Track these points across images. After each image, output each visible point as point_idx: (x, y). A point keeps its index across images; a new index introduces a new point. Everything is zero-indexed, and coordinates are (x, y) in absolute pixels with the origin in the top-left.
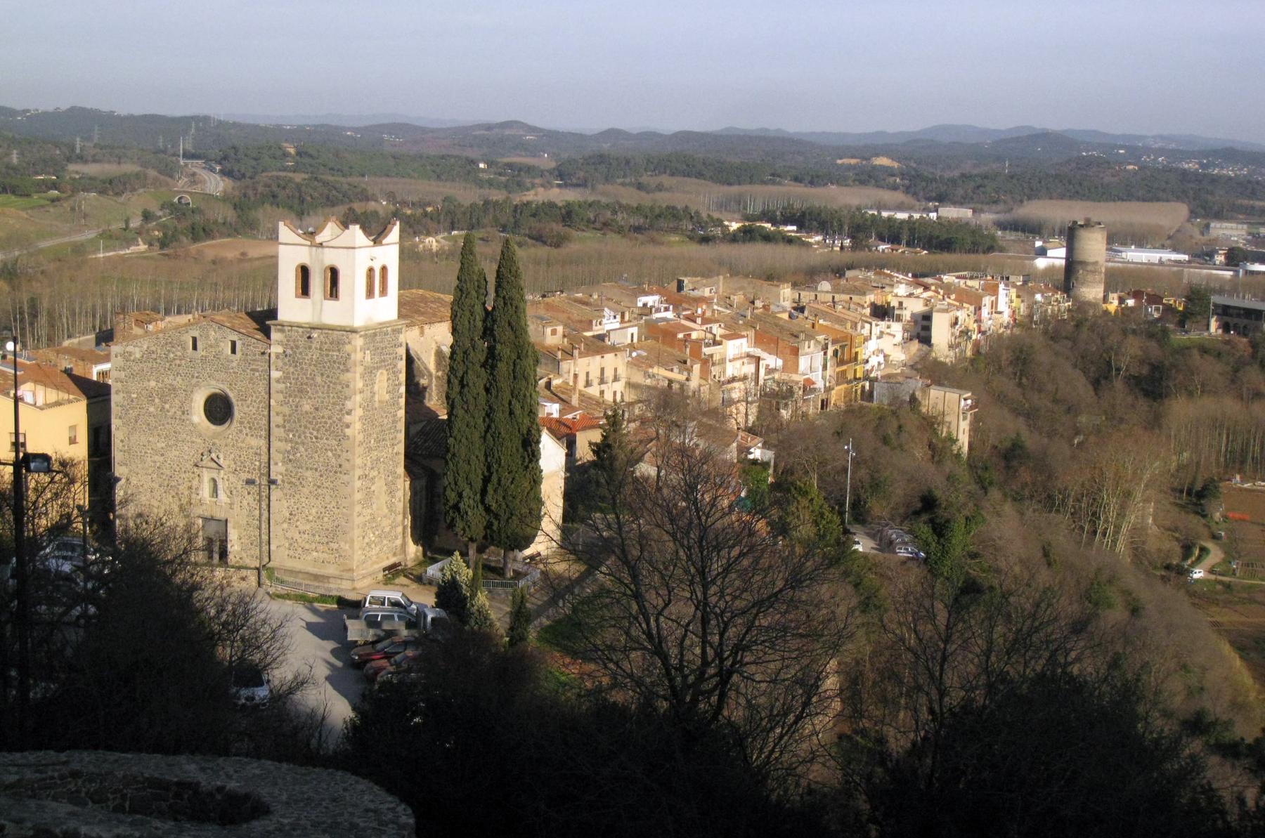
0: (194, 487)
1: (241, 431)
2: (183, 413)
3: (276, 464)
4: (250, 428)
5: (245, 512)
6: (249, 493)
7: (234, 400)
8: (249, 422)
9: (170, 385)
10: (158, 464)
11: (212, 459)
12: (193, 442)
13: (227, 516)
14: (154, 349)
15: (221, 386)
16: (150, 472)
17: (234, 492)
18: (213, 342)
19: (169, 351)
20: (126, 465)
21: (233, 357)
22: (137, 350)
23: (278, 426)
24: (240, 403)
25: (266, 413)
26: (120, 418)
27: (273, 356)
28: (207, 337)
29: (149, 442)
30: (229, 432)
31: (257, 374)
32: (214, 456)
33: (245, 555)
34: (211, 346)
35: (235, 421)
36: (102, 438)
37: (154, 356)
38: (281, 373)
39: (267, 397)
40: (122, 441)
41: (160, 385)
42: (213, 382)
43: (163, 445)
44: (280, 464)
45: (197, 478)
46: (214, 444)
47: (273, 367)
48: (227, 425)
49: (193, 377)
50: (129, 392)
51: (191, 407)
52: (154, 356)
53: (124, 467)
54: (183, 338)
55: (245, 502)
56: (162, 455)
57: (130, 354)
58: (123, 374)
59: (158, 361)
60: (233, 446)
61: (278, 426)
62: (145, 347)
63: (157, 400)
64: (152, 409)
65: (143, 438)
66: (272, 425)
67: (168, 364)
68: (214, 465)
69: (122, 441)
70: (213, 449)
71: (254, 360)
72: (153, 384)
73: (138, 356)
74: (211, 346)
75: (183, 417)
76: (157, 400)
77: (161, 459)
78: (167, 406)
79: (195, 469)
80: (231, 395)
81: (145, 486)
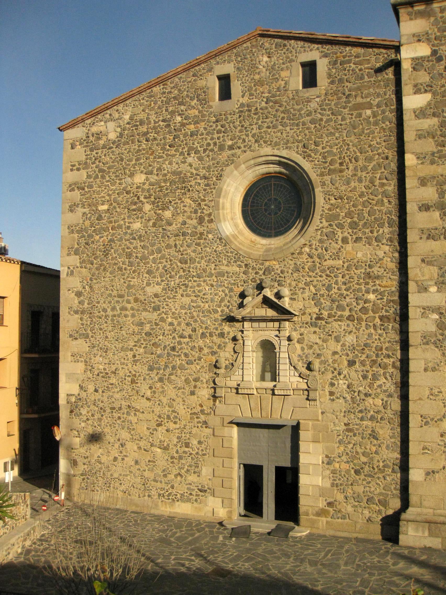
0: (223, 363)
1: (331, 236)
2: (201, 220)
3: (424, 289)
4: (354, 225)
5: (340, 404)
6: (351, 363)
7: (313, 176)
8: (349, 214)
9: (174, 173)
10: (147, 328)
11: (266, 301)
12: (221, 274)
13: (297, 417)
14: (143, 116)
15: (284, 153)
16: (132, 344)
17: (316, 365)
18: (265, 73)
19: (173, 113)
20: (87, 336)
21: (312, 92)
22: (111, 125)
23: (425, 208)
24: (327, 178)
25: (392, 187)
26: (76, 253)
27: (406, 66)
28: (253, 67)
29: (129, 287)
30: (302, 241)
31: (369, 112)
32: (269, 293)
33: (340, 497)
34: (260, 83)
35: (317, 217)
36: (45, 327)
37: (144, 129)
38: (428, 97)
39: (392, 154)
40: (79, 294)
41: (153, 178)
42: (268, 150)
43: (158, 289)
44: (433, 289)
45: (230, 345)
46: (267, 271)
47: (407, 89)
48: (294, 232)
49: (221, 148)
50: (93, 205)
51: (217, 207)
52: (144, 129)
53: (80, 341)
54: (201, 83)
55: (342, 384)
56: (156, 309)
57: (98, 136)
58: (84, 173)
59: (152, 135)
60: (312, 269)
61: (425, 208)
62: (127, 117)
63: (147, 207)
64: (137, 225)
65: (119, 283)
66: (411, 207)
67: (170, 138)
68: (271, 313)
69: (79, 294)
70: (267, 282)
71: (359, 89)
72: (140, 178)
73: (112, 136)
74: (260, 83)
75: (200, 229)
76: (147, 207)
77: (154, 316)
78: (168, 214)
79: (226, 328)
80: (306, 165)
81: (121, 373)
